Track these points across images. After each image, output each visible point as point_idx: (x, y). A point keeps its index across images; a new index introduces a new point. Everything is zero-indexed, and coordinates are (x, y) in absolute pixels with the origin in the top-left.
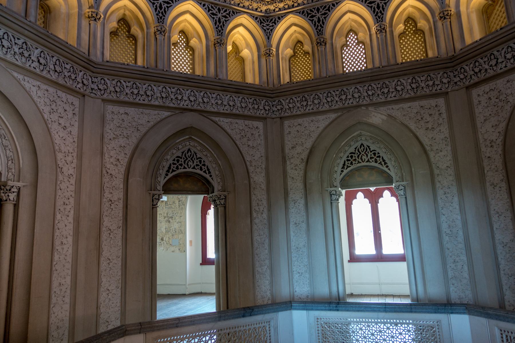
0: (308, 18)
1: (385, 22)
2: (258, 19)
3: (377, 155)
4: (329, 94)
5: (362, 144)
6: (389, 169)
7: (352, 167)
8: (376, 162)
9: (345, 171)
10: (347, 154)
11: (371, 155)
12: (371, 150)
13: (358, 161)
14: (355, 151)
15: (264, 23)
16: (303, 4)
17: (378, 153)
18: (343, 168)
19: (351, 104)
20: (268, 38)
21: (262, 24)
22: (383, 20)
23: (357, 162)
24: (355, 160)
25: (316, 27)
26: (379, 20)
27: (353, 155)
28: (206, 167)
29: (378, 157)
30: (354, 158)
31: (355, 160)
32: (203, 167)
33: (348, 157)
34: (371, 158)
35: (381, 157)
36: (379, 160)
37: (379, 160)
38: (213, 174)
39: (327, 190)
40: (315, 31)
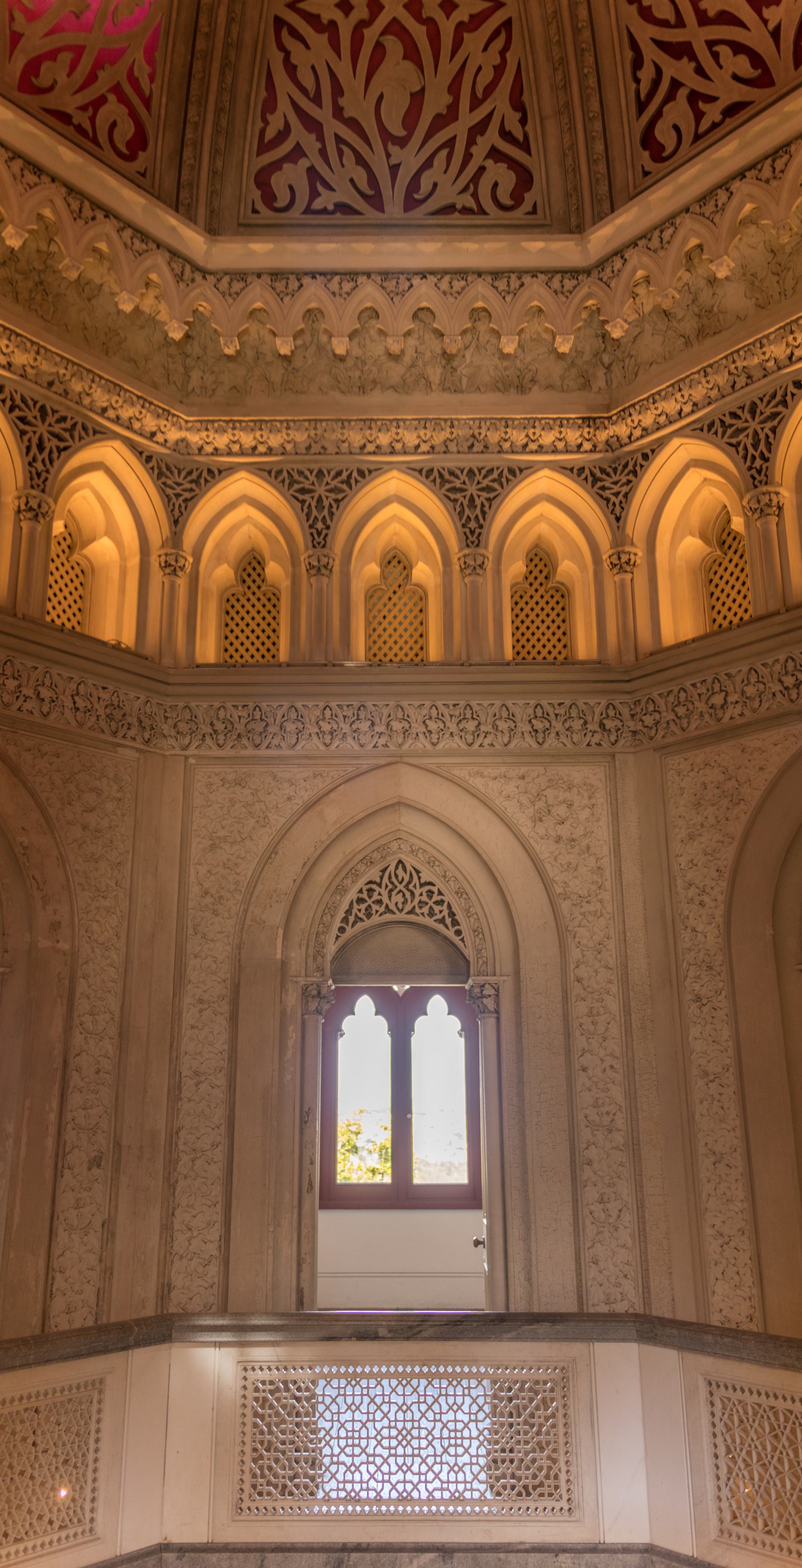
0: (291, 492)
1: (486, 547)
2: (153, 463)
3: (436, 897)
4: (328, 713)
5: (400, 862)
6: (462, 940)
7: (368, 923)
8: (431, 913)
9: (350, 932)
10: (361, 883)
11: (421, 895)
12: (422, 881)
13: (387, 906)
14: (382, 878)
15: (167, 477)
16: (282, 450)
17: (440, 893)
18: (345, 920)
19: (381, 748)
20: (176, 522)
21: (163, 479)
22: (482, 543)
23: (382, 909)
24: (379, 902)
25: (311, 522)
26: (471, 539)
27: (374, 886)
29: (437, 903)
31: (379, 902)
33: (361, 891)
34: (422, 904)
35: (446, 904)
36: (441, 912)
37: (441, 912)
39: (297, 982)
40: (308, 531)
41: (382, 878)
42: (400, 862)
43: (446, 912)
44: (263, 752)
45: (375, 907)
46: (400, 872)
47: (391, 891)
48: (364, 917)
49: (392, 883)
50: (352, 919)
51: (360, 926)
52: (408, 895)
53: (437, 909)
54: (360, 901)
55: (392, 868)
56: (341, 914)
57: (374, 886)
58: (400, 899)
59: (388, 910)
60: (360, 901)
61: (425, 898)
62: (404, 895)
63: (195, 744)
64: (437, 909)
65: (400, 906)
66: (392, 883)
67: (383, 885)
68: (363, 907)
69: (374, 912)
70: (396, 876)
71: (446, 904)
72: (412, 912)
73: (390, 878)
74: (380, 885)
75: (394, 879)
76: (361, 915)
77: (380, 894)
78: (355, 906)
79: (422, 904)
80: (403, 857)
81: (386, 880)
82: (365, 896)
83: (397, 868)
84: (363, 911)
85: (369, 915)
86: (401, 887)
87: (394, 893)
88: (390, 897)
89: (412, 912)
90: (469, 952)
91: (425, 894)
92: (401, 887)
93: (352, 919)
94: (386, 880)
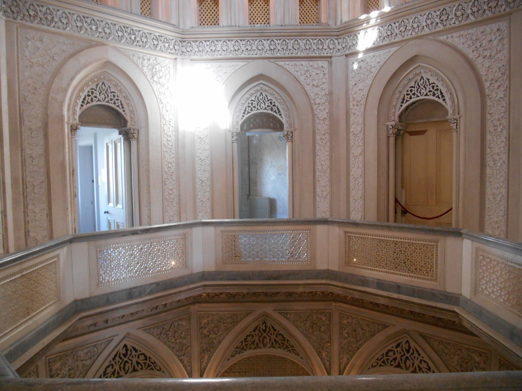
3: (116, 98)
6: (125, 114)
8: (115, 103)
11: (111, 96)
13: (99, 99)
14: (96, 87)
18: (83, 102)
24: (96, 97)
28: (276, 107)
30: (94, 95)
32: (273, 107)
35: (120, 101)
36: (118, 103)
37: (118, 103)
38: (282, 113)
41: (96, 87)
42: (103, 83)
43: (120, 103)
44: (51, 29)
45: (94, 99)
46: (103, 86)
47: (100, 93)
48: (90, 102)
49: (100, 90)
50: (86, 102)
51: (89, 105)
52: (106, 95)
53: (117, 102)
54: (89, 96)
55: (100, 85)
56: (82, 100)
57: (94, 91)
58: (103, 96)
59: (99, 100)
60: (89, 96)
61: (112, 97)
62: (105, 95)
63: (19, 18)
64: (117, 102)
65: (104, 99)
66: (100, 90)
67: (97, 91)
68: (90, 98)
69: (94, 100)
70: (102, 88)
71: (120, 101)
72: (108, 102)
73: (100, 88)
74: (96, 90)
75: (101, 89)
76: (89, 101)
77: (96, 94)
78: (87, 97)
79: (111, 100)
80: (105, 81)
81: (98, 89)
82: (90, 94)
83: (102, 85)
84: (90, 99)
85: (92, 101)
86: (104, 92)
87: (101, 94)
88: (100, 95)
89: (108, 102)
90: (128, 118)
91: (112, 96)
92: (104, 92)
93: (86, 102)
94: (98, 89)
